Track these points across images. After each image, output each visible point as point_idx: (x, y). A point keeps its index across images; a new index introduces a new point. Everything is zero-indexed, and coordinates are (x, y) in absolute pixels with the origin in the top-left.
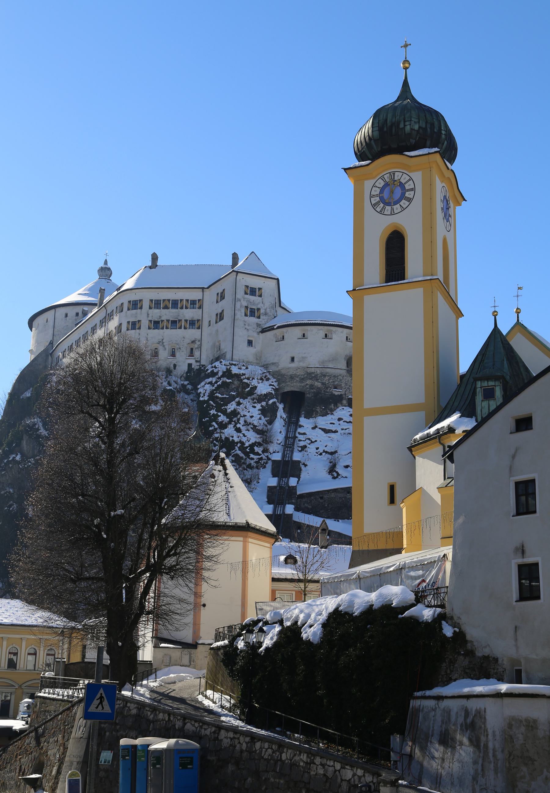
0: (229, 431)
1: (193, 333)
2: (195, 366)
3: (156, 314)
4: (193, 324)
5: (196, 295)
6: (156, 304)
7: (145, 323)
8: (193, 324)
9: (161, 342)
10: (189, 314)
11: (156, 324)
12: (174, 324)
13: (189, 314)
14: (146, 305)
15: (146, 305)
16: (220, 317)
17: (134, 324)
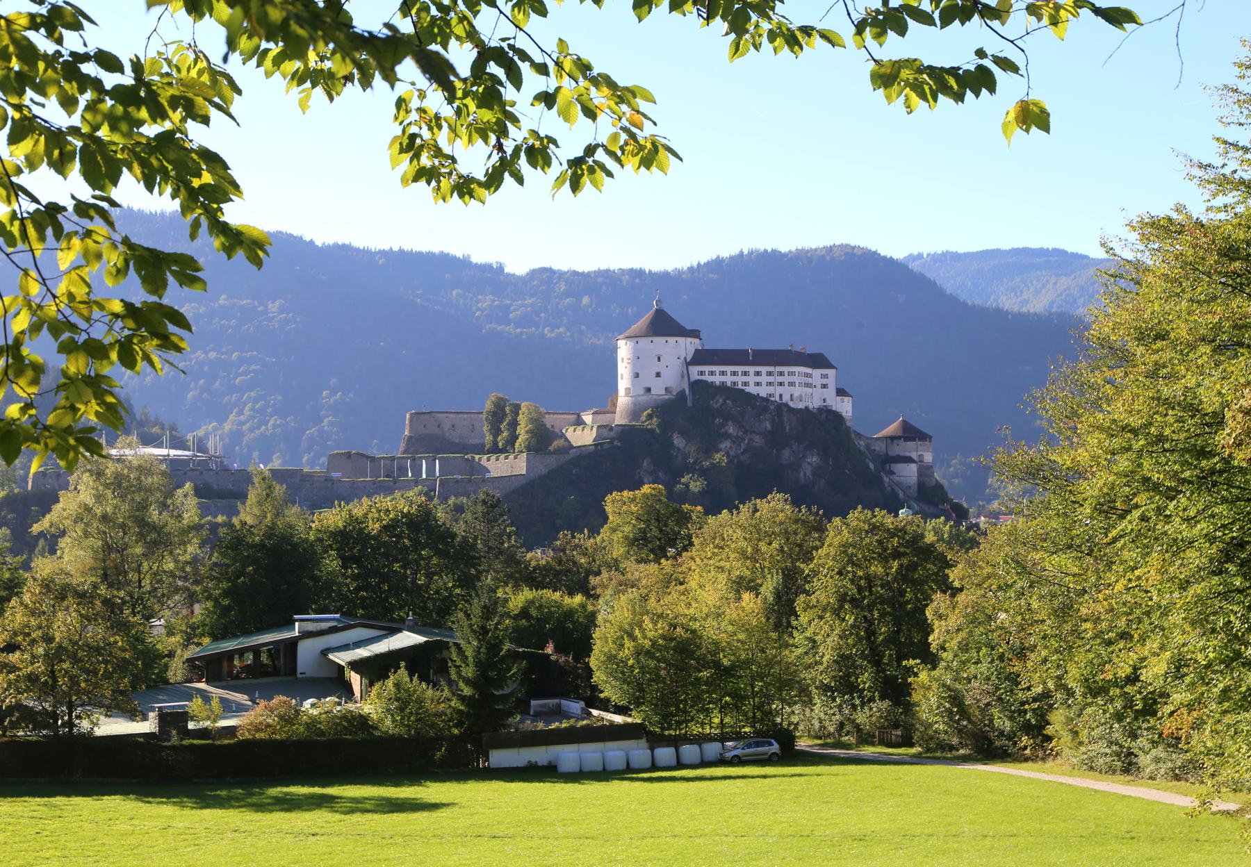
16: (824, 386)
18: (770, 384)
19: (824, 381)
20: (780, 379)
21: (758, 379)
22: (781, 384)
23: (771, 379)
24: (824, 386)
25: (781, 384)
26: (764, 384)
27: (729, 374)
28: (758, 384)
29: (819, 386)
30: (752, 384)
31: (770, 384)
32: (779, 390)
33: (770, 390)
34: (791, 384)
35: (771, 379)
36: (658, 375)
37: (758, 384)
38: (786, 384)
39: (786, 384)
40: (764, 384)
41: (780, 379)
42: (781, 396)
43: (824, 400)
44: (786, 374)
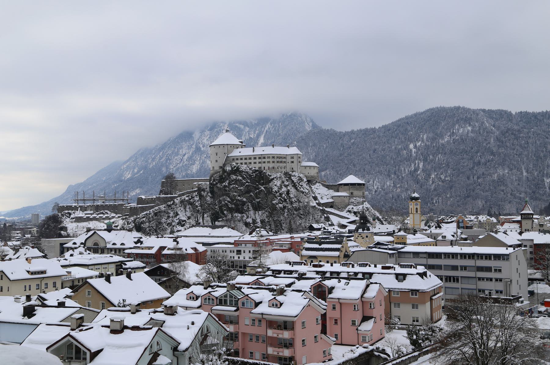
0: (302, 189)
1: (285, 164)
2: (286, 172)
3: (278, 160)
4: (285, 162)
5: (285, 156)
6: (278, 157)
7: (276, 162)
8: (285, 162)
9: (279, 166)
10: (284, 160)
11: (278, 162)
12: (281, 162)
13: (284, 160)
14: (276, 157)
15: (276, 157)
16: (292, 162)
17: (273, 162)
18: (260, 163)
19: (292, 160)
20: (264, 160)
21: (255, 161)
22: (264, 162)
23: (260, 160)
24: (292, 162)
25: (264, 162)
26: (257, 163)
27: (244, 159)
28: (255, 163)
29: (290, 162)
30: (252, 163)
31: (260, 163)
32: (264, 165)
33: (260, 165)
34: (269, 162)
35: (260, 160)
36: (217, 161)
37: (255, 163)
38: (266, 162)
39: (266, 162)
40: (257, 163)
41: (264, 160)
42: (264, 167)
43: (293, 169)
44: (266, 158)
